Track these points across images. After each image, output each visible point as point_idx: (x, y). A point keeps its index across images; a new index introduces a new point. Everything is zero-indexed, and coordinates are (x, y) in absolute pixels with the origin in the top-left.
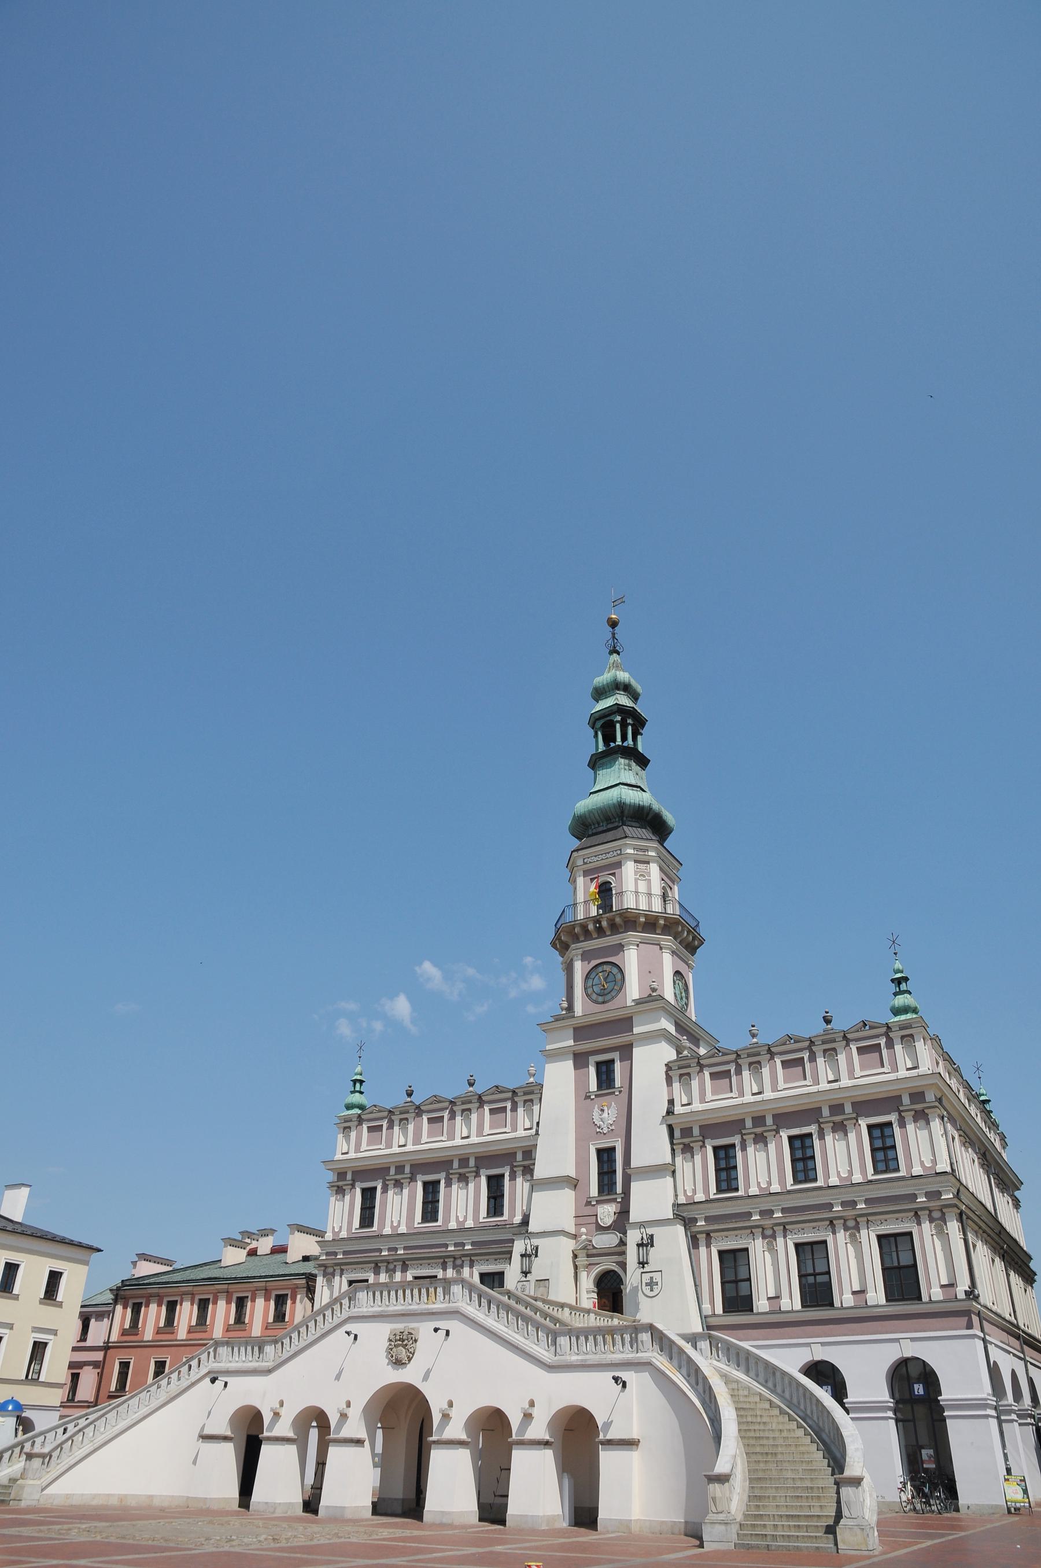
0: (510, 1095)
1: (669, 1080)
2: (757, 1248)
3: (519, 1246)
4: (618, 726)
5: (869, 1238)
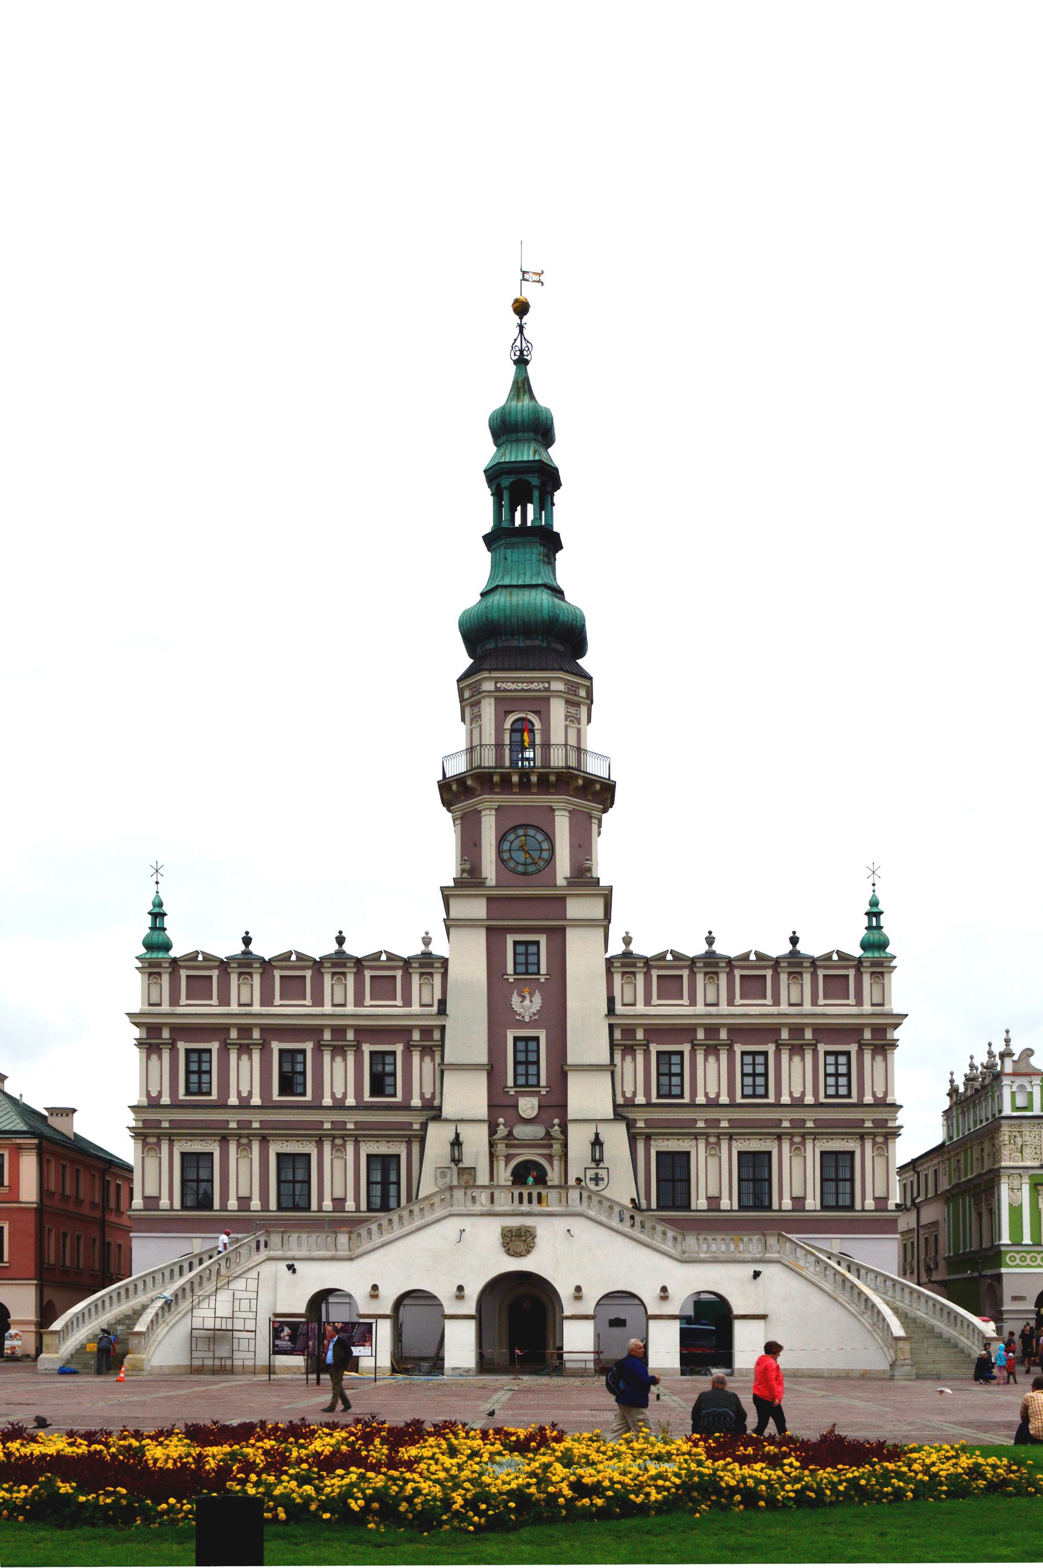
0: (402, 964)
1: (609, 974)
2: (698, 1152)
3: (438, 1137)
4: (536, 494)
5: (812, 1152)
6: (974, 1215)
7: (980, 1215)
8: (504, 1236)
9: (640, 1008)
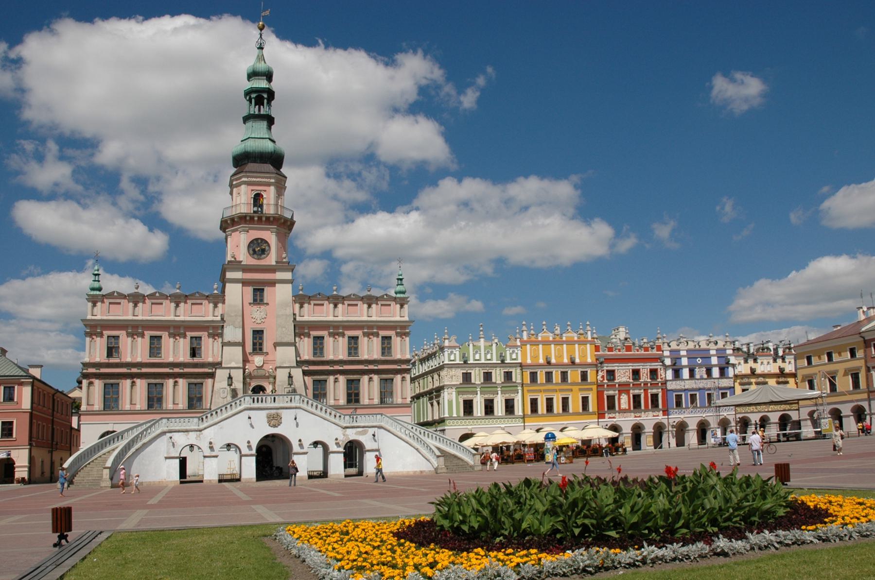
6: (429, 405)
7: (432, 405)
8: (268, 418)
9: (306, 318)
